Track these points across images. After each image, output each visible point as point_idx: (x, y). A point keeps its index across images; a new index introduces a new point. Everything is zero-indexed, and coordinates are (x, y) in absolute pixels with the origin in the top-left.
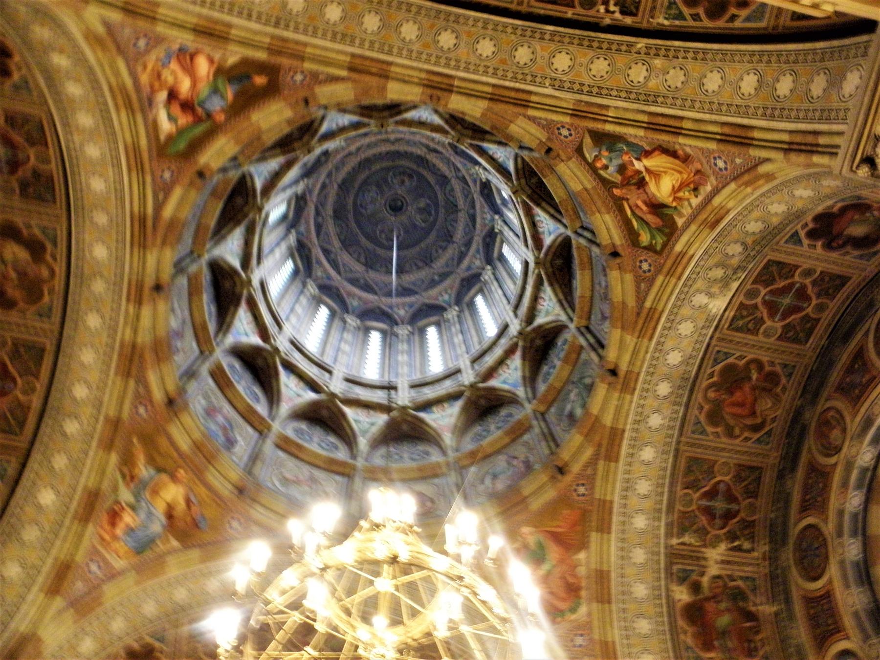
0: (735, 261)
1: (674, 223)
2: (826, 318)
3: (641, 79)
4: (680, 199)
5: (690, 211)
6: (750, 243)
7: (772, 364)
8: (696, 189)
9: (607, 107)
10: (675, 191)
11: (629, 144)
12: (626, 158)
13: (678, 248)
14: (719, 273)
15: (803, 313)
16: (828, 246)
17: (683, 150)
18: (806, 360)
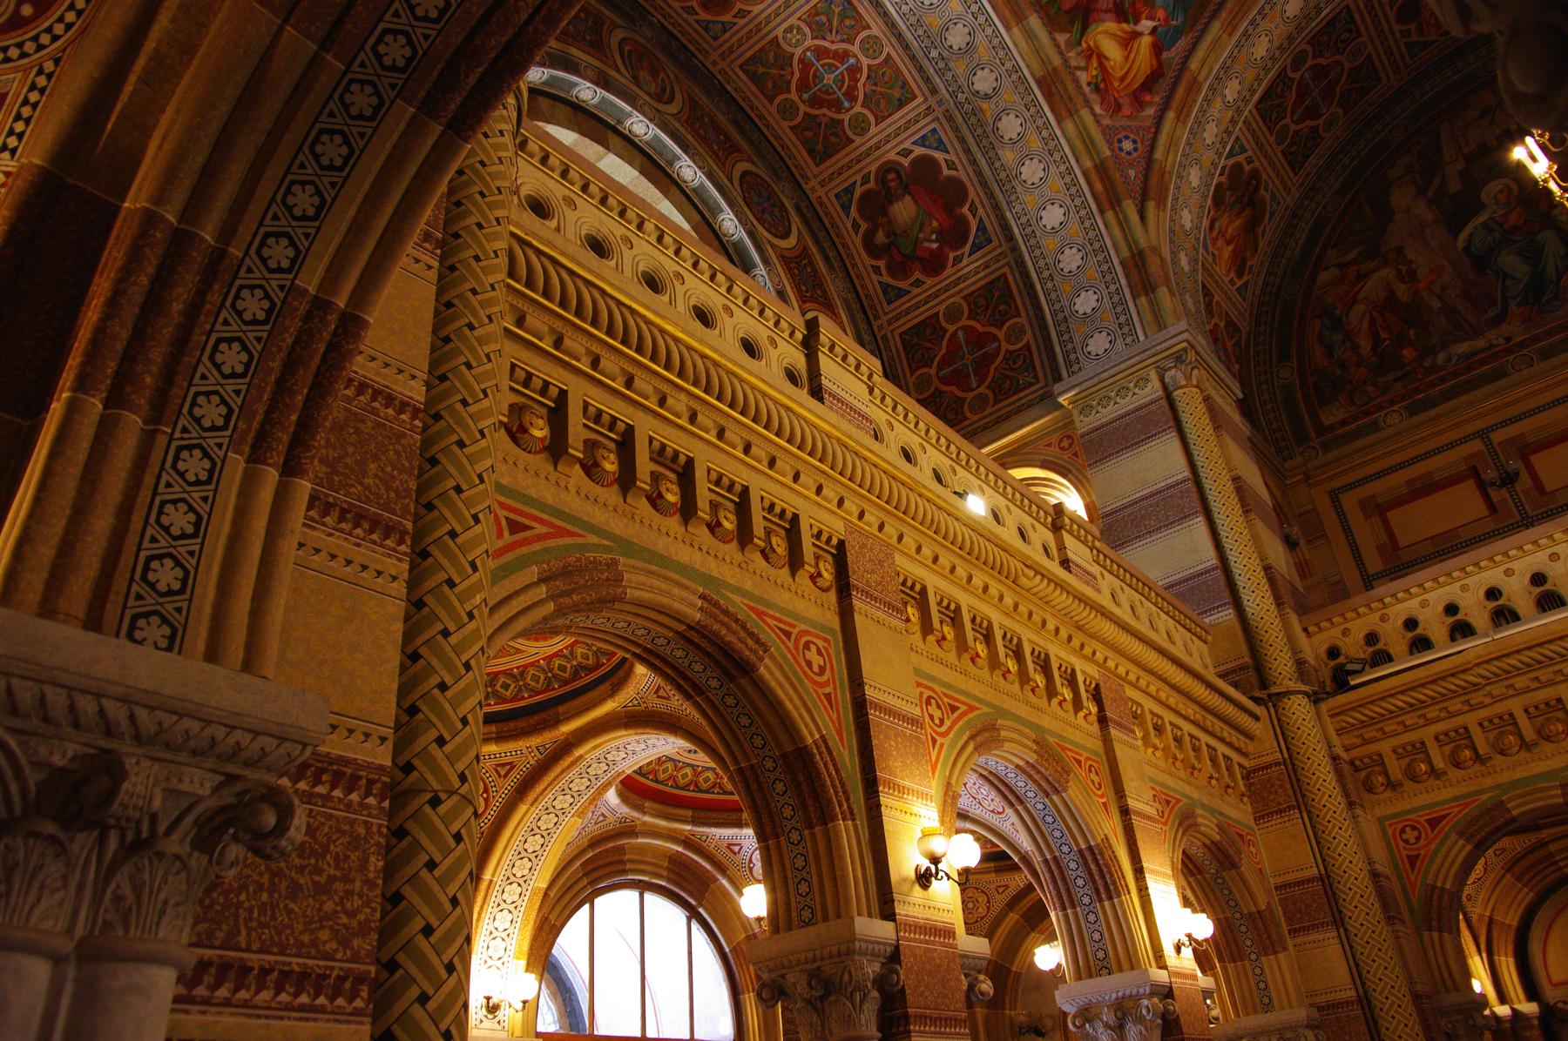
0: (960, 68)
1: (1063, 31)
2: (770, 112)
3: (1227, 92)
4: (1089, 58)
5: (1073, 63)
6: (985, 106)
7: (742, 14)
8: (1097, 89)
9: (1230, 35)
10: (1102, 57)
11: (1178, 33)
12: (1161, 14)
13: (1034, 21)
14: (957, 38)
15: (793, 88)
16: (889, 168)
17: (1150, 104)
18: (715, 56)
